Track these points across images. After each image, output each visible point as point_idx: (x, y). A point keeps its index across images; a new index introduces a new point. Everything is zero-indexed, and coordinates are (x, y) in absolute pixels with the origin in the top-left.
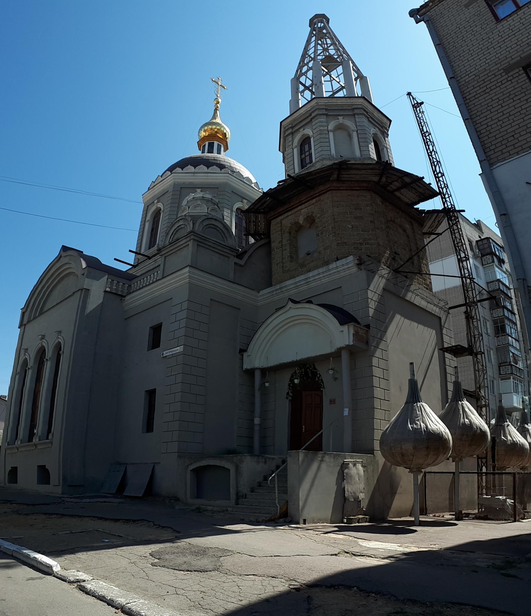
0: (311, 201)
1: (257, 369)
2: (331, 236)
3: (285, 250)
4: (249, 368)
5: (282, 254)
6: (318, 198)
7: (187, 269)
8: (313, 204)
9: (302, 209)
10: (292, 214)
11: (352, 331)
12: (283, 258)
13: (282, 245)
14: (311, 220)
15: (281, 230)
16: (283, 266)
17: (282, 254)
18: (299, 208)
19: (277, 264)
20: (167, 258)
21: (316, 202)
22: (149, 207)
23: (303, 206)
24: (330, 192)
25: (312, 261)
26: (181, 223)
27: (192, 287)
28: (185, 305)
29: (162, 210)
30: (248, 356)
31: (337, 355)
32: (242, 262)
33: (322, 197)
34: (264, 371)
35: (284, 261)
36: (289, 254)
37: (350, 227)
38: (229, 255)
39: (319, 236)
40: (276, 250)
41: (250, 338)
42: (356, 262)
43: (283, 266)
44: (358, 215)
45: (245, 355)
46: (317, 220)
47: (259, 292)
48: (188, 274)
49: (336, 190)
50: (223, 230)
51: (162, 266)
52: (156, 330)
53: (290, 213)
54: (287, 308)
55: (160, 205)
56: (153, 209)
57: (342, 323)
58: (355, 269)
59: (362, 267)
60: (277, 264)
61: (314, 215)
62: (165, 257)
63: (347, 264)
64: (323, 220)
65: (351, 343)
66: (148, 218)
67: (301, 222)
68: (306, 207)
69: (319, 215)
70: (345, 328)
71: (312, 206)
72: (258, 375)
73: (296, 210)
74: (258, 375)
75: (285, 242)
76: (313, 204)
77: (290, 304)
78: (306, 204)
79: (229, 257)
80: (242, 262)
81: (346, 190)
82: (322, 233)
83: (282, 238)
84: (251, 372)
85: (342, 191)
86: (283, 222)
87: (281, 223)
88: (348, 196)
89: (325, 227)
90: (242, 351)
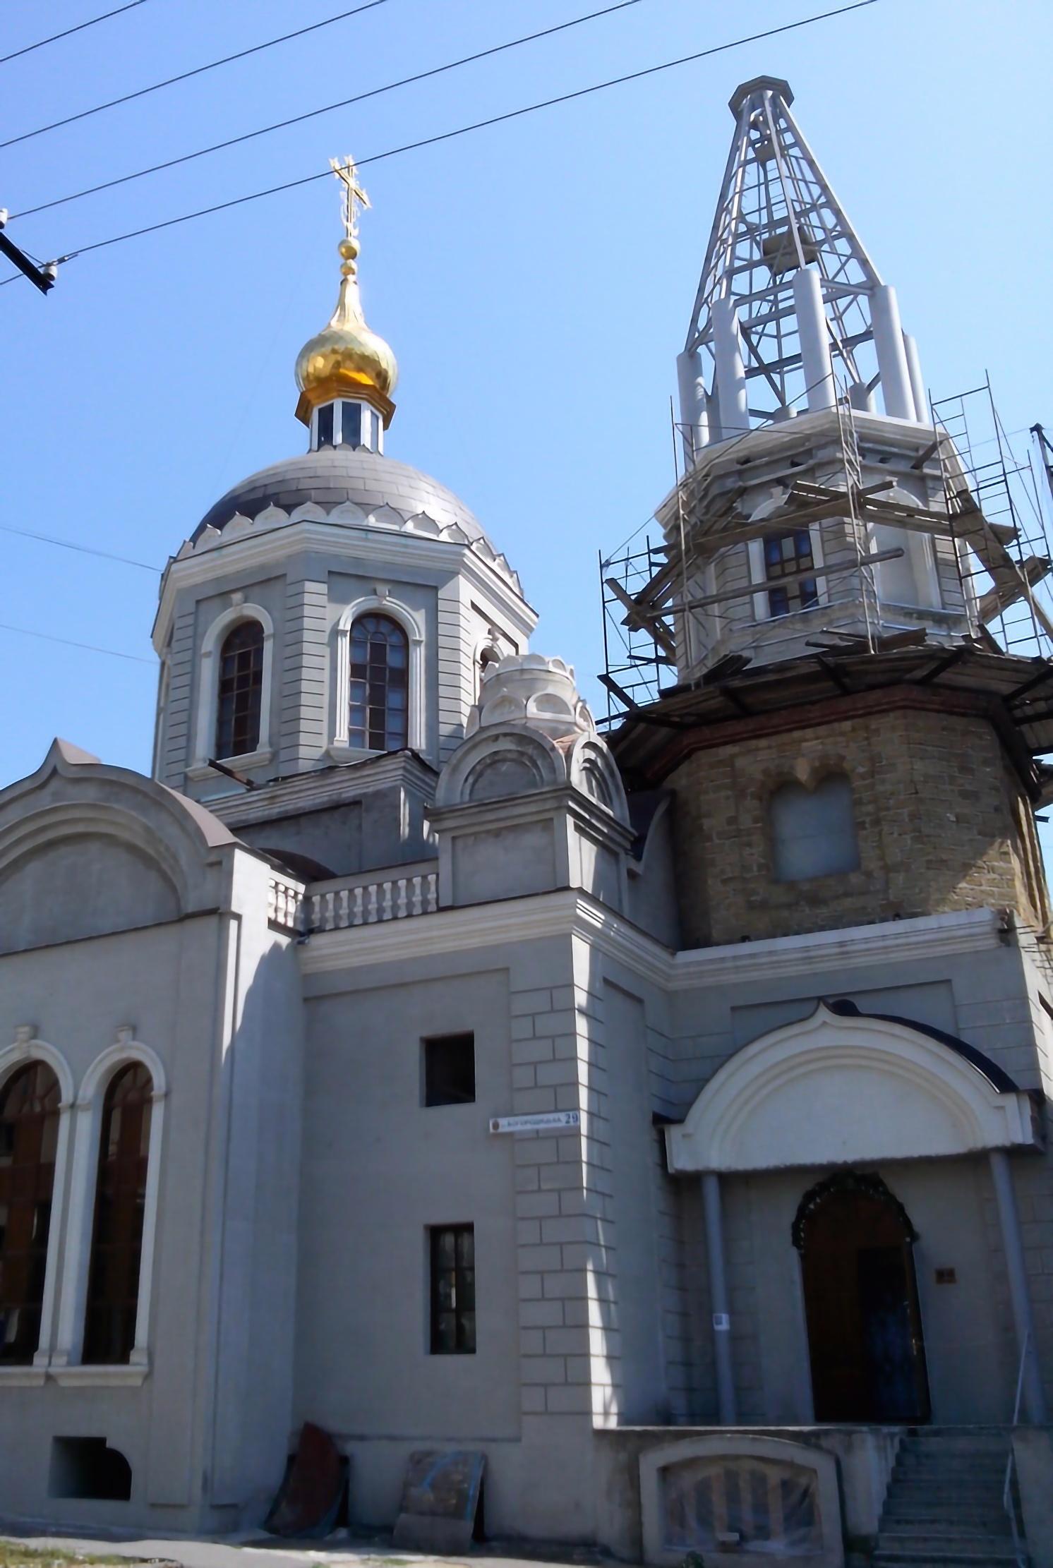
0: (836, 725)
2: (908, 837)
9: (806, 740)
10: (769, 747)
18: (797, 734)
19: (725, 882)
23: (809, 733)
24: (899, 713)
29: (268, 628)
31: (976, 1161)
32: (639, 868)
33: (874, 723)
34: (729, 1180)
36: (762, 861)
37: (953, 819)
39: (865, 829)
40: (717, 841)
44: (968, 787)
47: (673, 954)
50: (606, 774)
55: (253, 610)
56: (224, 619)
60: (725, 882)
61: (847, 766)
62: (454, 838)
68: (817, 738)
69: (861, 770)
71: (840, 739)
72: (711, 1190)
73: (785, 738)
74: (711, 1190)
75: (746, 822)
76: (842, 734)
77: (824, 1014)
78: (822, 730)
81: (938, 711)
82: (877, 822)
88: (944, 729)
89: (888, 809)
90: (661, 1122)
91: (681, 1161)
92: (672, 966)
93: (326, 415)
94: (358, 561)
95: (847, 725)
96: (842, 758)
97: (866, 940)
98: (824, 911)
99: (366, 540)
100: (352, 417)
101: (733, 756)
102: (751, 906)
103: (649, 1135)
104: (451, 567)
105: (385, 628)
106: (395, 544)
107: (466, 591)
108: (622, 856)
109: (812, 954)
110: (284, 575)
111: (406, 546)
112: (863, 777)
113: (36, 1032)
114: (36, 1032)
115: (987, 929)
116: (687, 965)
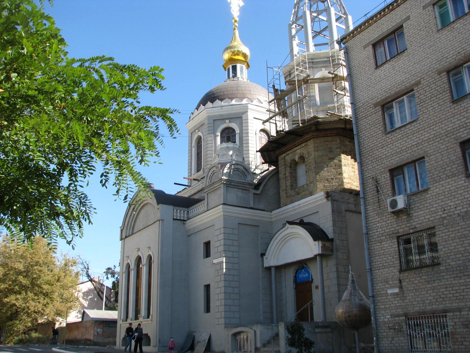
0: (302, 145)
1: (272, 267)
3: (288, 180)
4: (267, 266)
5: (286, 183)
6: (305, 143)
7: (221, 205)
8: (303, 147)
11: (320, 245)
12: (286, 187)
13: (286, 177)
14: (302, 158)
15: (285, 164)
16: (286, 193)
17: (286, 183)
18: (295, 149)
20: (209, 194)
21: (305, 146)
22: (193, 134)
23: (297, 148)
25: (303, 191)
26: (215, 169)
27: (226, 218)
28: (222, 231)
30: (266, 258)
35: (287, 189)
38: (249, 189)
41: (268, 244)
42: (325, 195)
43: (286, 193)
44: (331, 156)
45: (265, 257)
46: (306, 160)
47: (271, 212)
48: (222, 210)
49: (317, 137)
50: (244, 170)
51: (206, 199)
52: (207, 245)
53: (289, 152)
54: (286, 227)
55: (200, 134)
56: (195, 137)
57: (315, 239)
58: (325, 200)
59: (330, 198)
61: (304, 156)
62: (208, 194)
63: (320, 196)
64: (309, 161)
65: (320, 253)
66: (193, 144)
67: (297, 160)
69: (307, 156)
70: (317, 243)
71: (303, 148)
72: (273, 270)
73: (293, 150)
74: (273, 270)
75: (287, 174)
76: (303, 147)
77: (288, 225)
78: (299, 147)
79: (249, 190)
80: (258, 192)
81: (324, 137)
83: (285, 172)
84: (269, 269)
85: (321, 138)
86: (286, 158)
87: (285, 159)
88: (325, 141)
90: (263, 255)
91: (266, 265)
92: (271, 215)
93: (229, 69)
94: (221, 115)
95: (303, 145)
96: (303, 154)
97: (303, 203)
98: (299, 196)
99: (222, 109)
100: (234, 68)
101: (285, 157)
102: (287, 197)
103: (260, 258)
104: (245, 110)
105: (227, 131)
106: (229, 108)
107: (251, 115)
108: (251, 190)
109: (295, 208)
110: (204, 124)
111: (232, 108)
112: (307, 158)
113: (139, 250)
114: (139, 250)
115: (323, 197)
116: (276, 214)
